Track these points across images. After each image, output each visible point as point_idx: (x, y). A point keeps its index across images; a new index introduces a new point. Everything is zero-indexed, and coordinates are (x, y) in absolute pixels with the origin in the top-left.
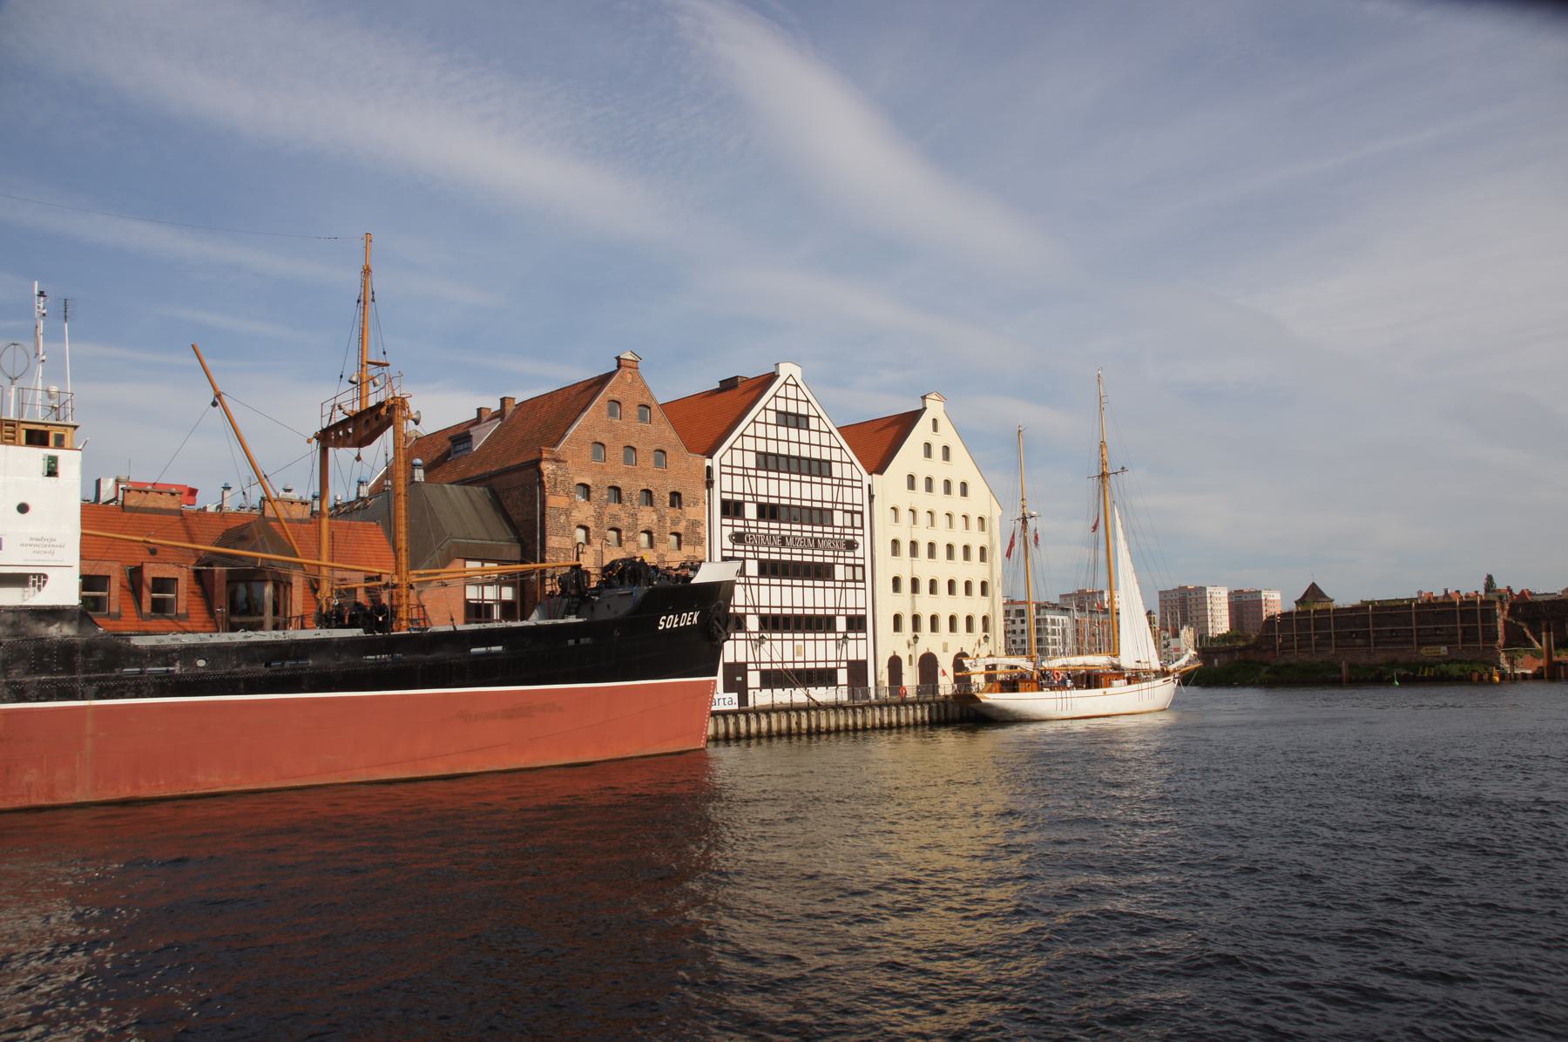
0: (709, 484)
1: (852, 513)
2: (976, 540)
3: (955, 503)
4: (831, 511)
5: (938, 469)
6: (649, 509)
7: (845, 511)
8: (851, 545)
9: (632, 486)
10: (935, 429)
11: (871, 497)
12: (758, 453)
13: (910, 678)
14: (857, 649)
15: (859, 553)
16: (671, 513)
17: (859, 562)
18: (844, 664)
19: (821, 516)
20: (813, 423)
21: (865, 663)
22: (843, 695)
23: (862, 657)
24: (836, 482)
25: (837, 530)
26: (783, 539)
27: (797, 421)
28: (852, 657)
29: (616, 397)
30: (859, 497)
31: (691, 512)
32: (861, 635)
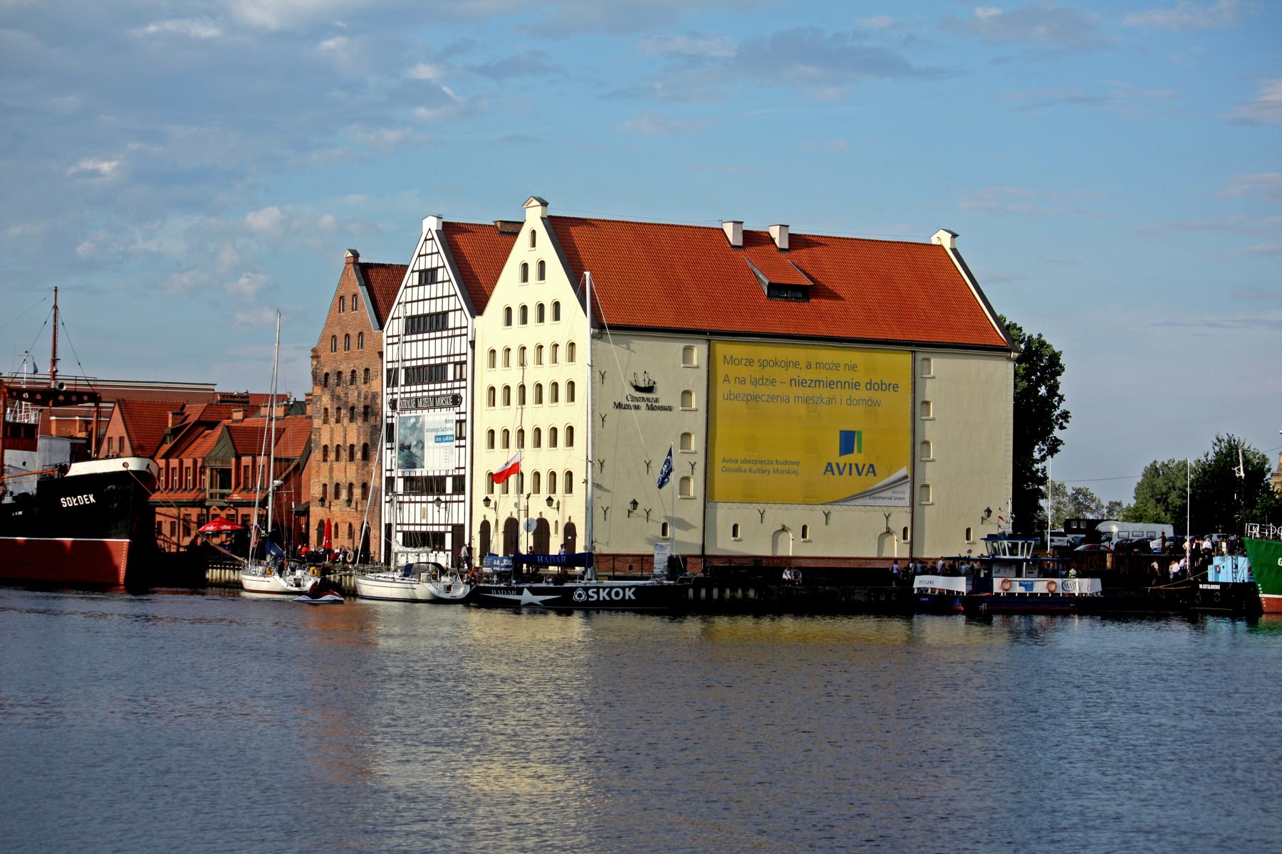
0: (381, 354)
1: (462, 363)
2: (562, 373)
3: (548, 332)
4: (446, 364)
5: (534, 293)
6: (353, 387)
7: (455, 364)
8: (456, 400)
9: (346, 369)
10: (534, 245)
11: (473, 343)
12: (407, 318)
13: (497, 544)
14: (458, 514)
15: (463, 405)
16: (364, 388)
17: (463, 417)
18: (450, 528)
19: (434, 373)
20: (441, 275)
21: (463, 526)
22: (444, 559)
23: (461, 522)
24: (450, 333)
25: (450, 385)
26: (417, 399)
27: (428, 277)
28: (455, 522)
29: (342, 293)
30: (461, 345)
31: (375, 385)
32: (462, 497)
